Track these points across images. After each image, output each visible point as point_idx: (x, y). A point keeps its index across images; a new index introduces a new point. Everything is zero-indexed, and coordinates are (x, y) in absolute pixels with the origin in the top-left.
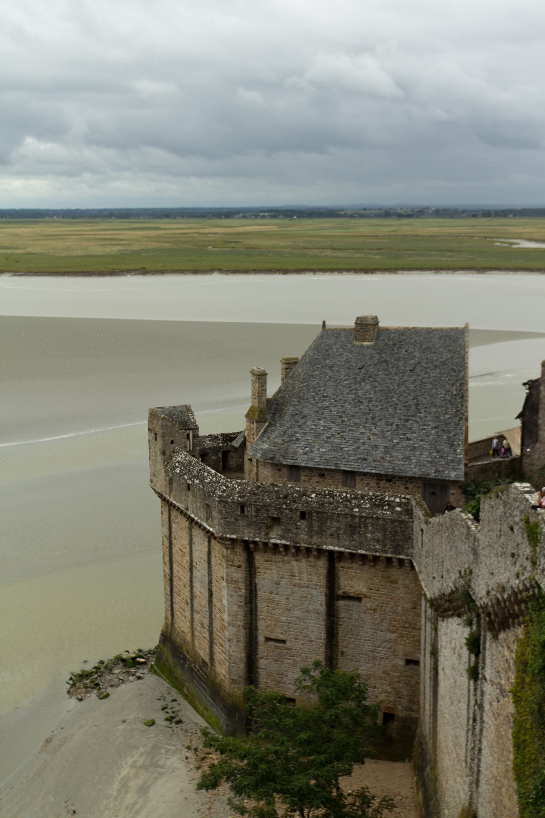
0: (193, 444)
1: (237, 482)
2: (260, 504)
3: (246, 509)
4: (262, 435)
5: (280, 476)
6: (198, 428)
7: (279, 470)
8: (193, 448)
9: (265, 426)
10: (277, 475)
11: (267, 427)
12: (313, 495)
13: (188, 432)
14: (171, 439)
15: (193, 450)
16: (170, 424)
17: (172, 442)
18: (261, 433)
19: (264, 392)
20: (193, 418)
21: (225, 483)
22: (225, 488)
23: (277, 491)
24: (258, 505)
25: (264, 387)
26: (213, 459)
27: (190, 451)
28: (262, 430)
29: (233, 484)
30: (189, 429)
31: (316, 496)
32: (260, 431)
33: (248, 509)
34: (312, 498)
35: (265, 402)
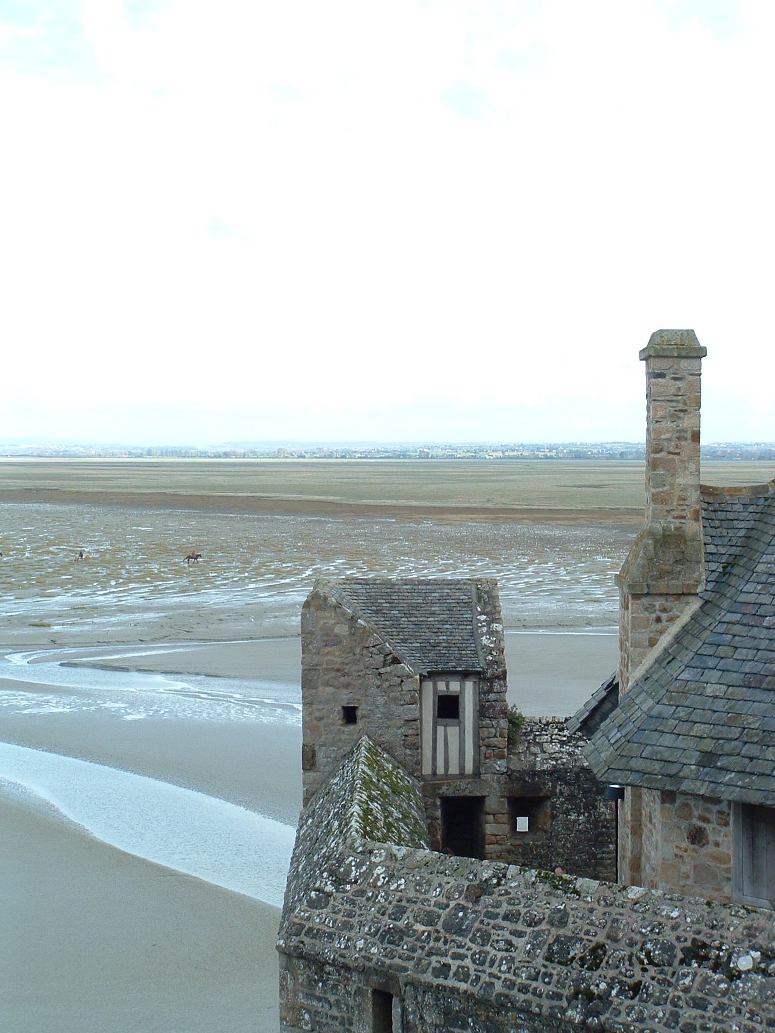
0: (477, 747)
1: (392, 856)
2: (463, 986)
3: (396, 1012)
4: (658, 661)
5: (703, 874)
6: (503, 676)
7: (697, 837)
8: (477, 764)
9: (685, 619)
10: (686, 868)
11: (694, 618)
12: (744, 963)
13: (455, 686)
14: (345, 698)
15: (477, 774)
16: (342, 630)
17: (350, 715)
18: (657, 651)
19: (687, 444)
20: (491, 633)
21: (340, 861)
22: (329, 888)
23: (561, 919)
24: (454, 990)
25: (686, 422)
26: (569, 826)
27: (462, 775)
28: (665, 640)
29: (374, 865)
30: (465, 675)
31: (757, 970)
32: (652, 643)
33: (404, 1009)
34: (733, 976)
35: (694, 496)
